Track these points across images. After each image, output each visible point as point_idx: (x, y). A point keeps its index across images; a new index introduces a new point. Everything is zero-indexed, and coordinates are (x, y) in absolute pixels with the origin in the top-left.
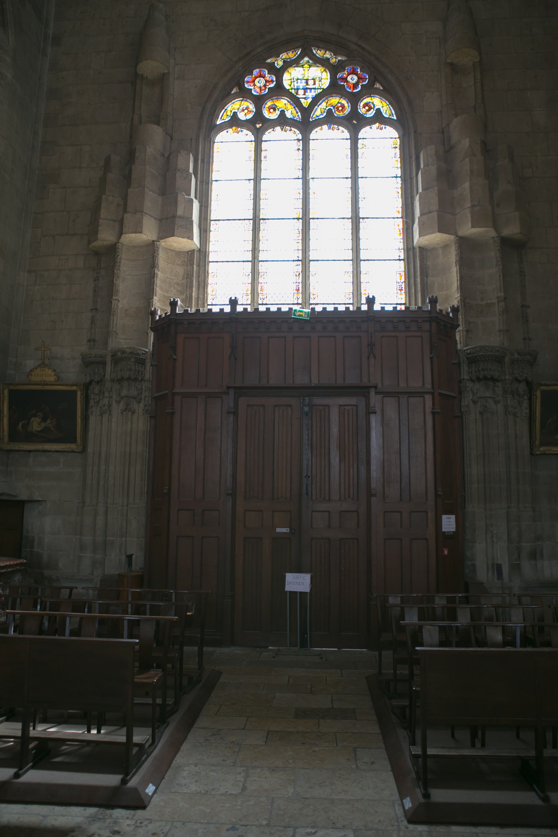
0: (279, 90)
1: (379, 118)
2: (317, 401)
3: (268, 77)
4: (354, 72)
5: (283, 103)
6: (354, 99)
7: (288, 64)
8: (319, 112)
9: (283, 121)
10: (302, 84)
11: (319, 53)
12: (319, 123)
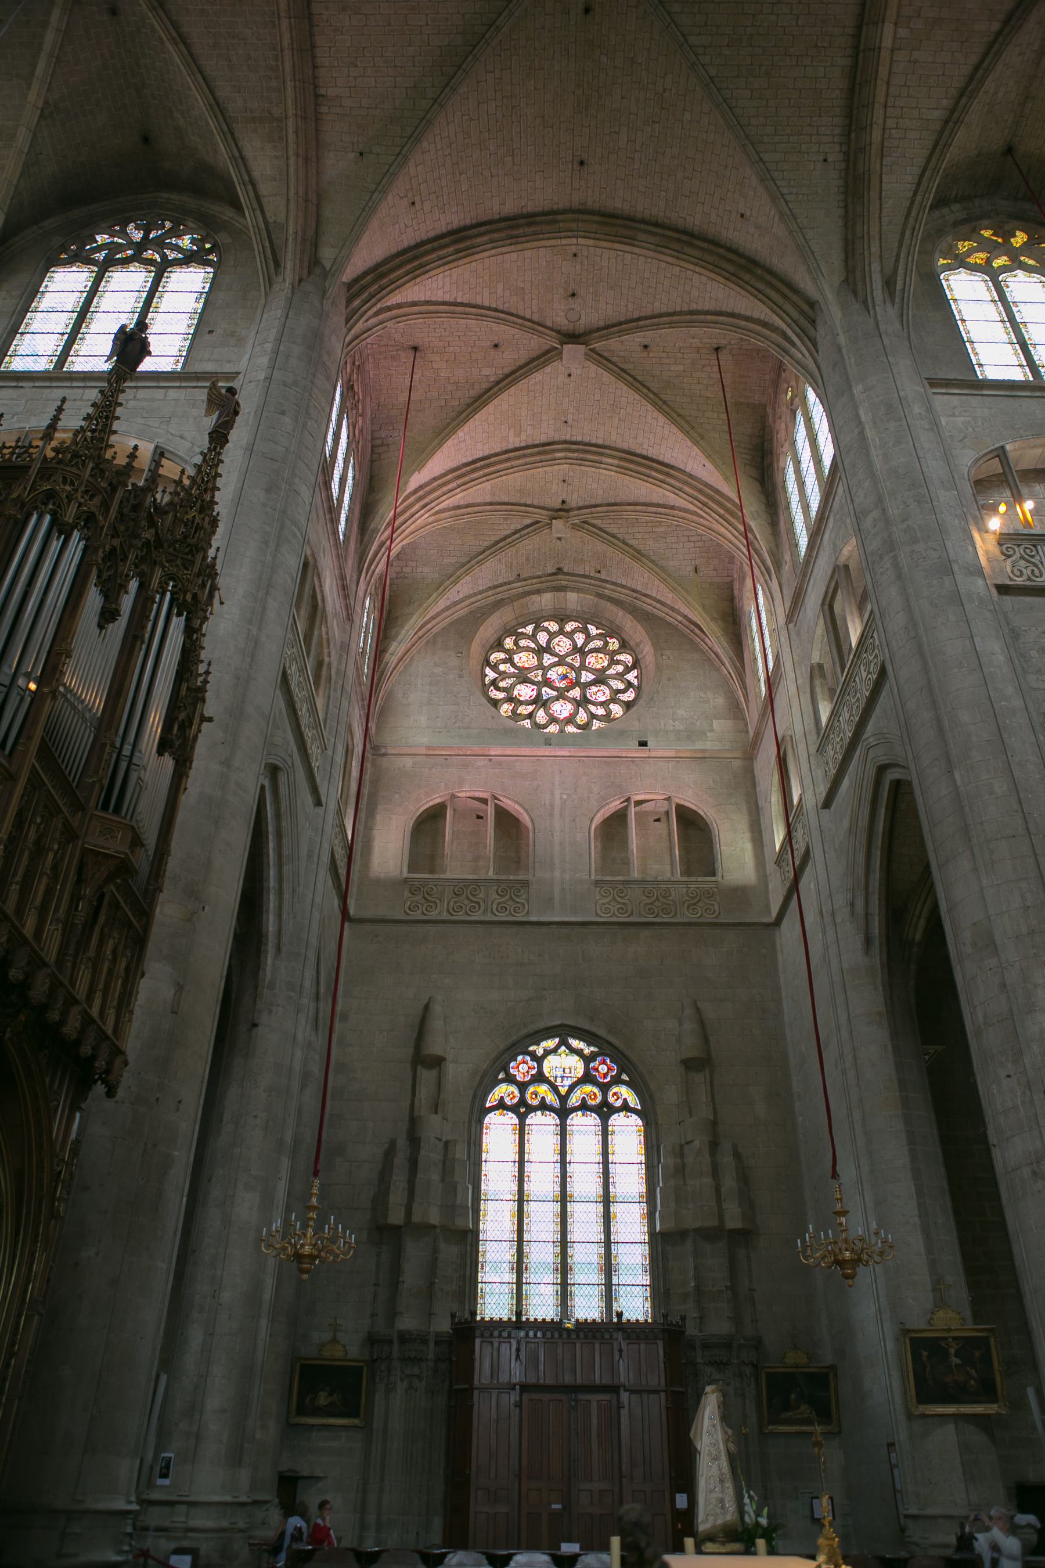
0: (540, 1078)
1: (626, 1107)
2: (581, 1397)
3: (531, 1063)
4: (604, 1062)
5: (543, 1089)
6: (605, 1088)
7: (547, 1053)
8: (574, 1100)
9: (543, 1107)
10: (560, 1073)
11: (575, 1043)
12: (575, 1109)
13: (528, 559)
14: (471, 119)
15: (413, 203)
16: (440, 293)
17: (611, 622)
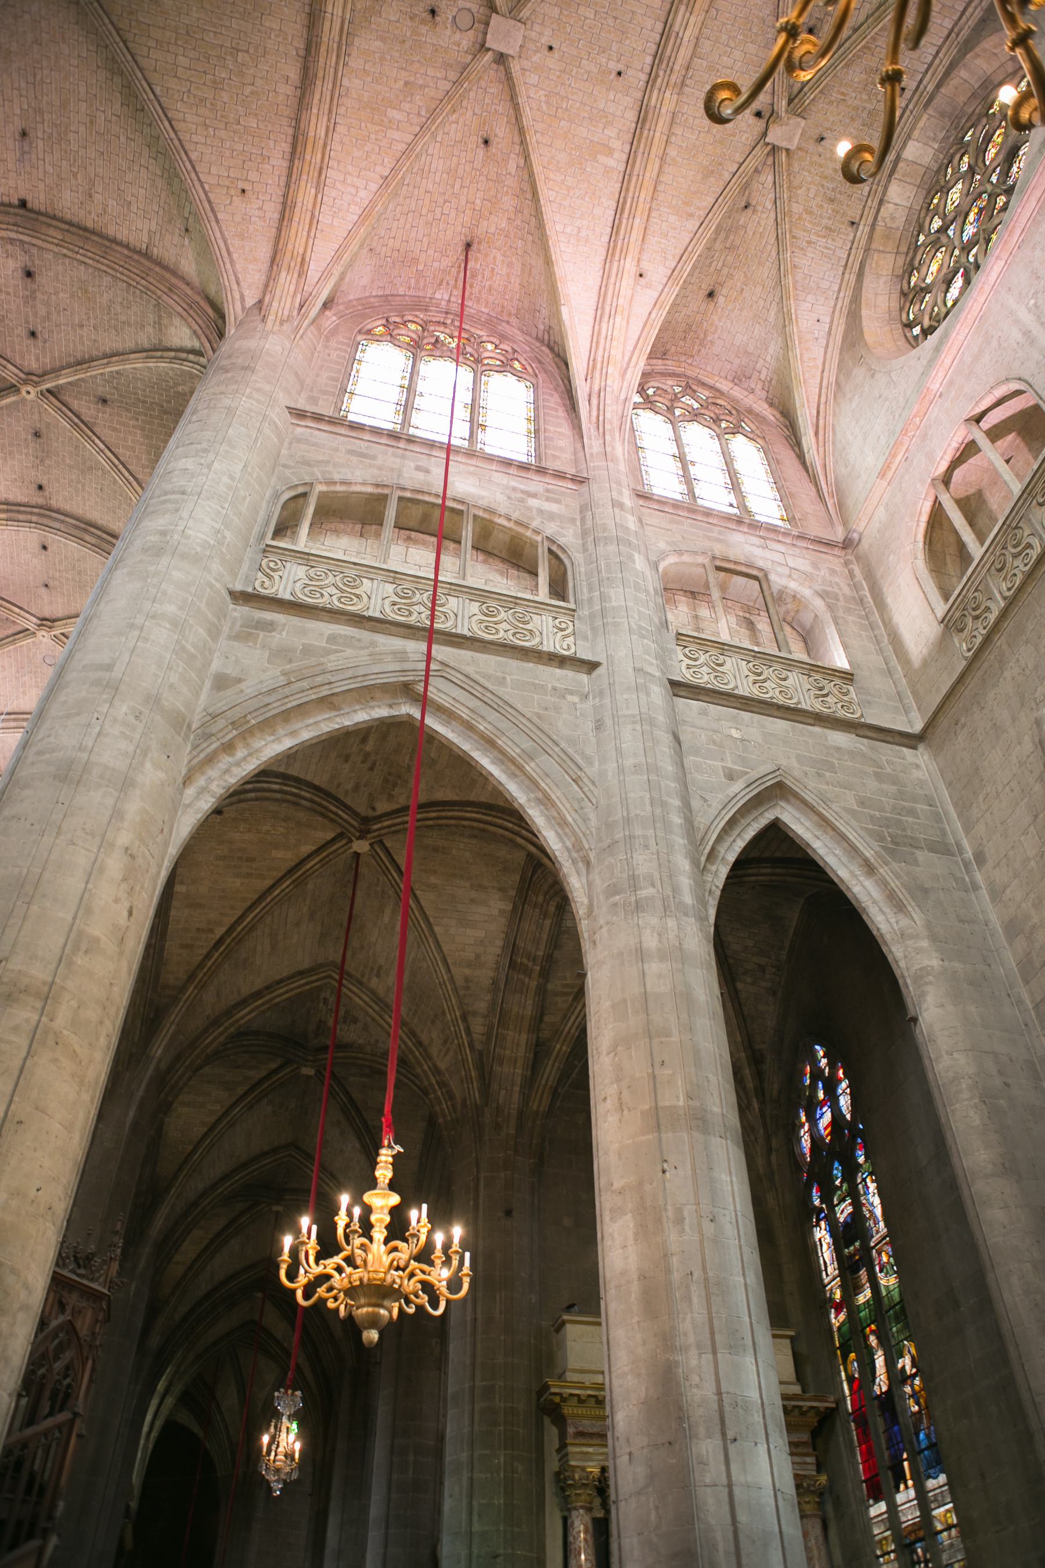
13: (832, 201)
14: (189, 91)
15: (243, 191)
16: (362, 194)
17: (974, 95)
